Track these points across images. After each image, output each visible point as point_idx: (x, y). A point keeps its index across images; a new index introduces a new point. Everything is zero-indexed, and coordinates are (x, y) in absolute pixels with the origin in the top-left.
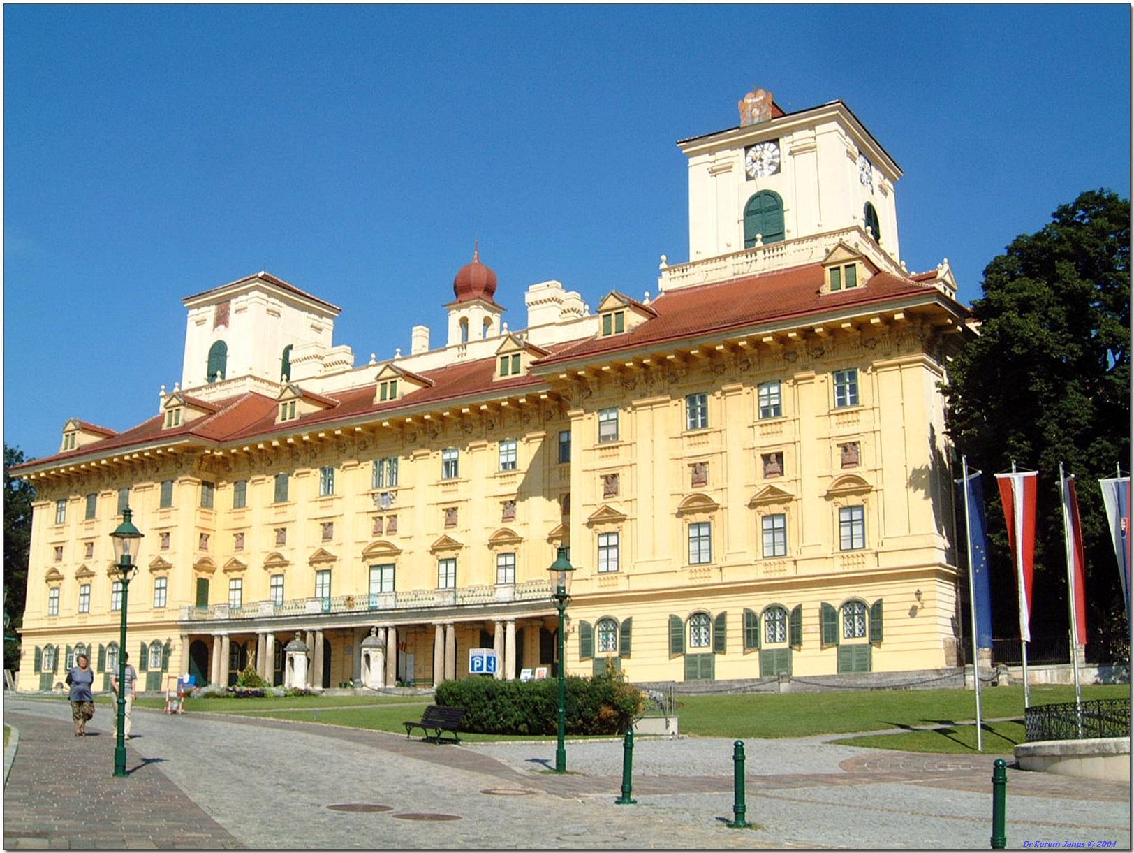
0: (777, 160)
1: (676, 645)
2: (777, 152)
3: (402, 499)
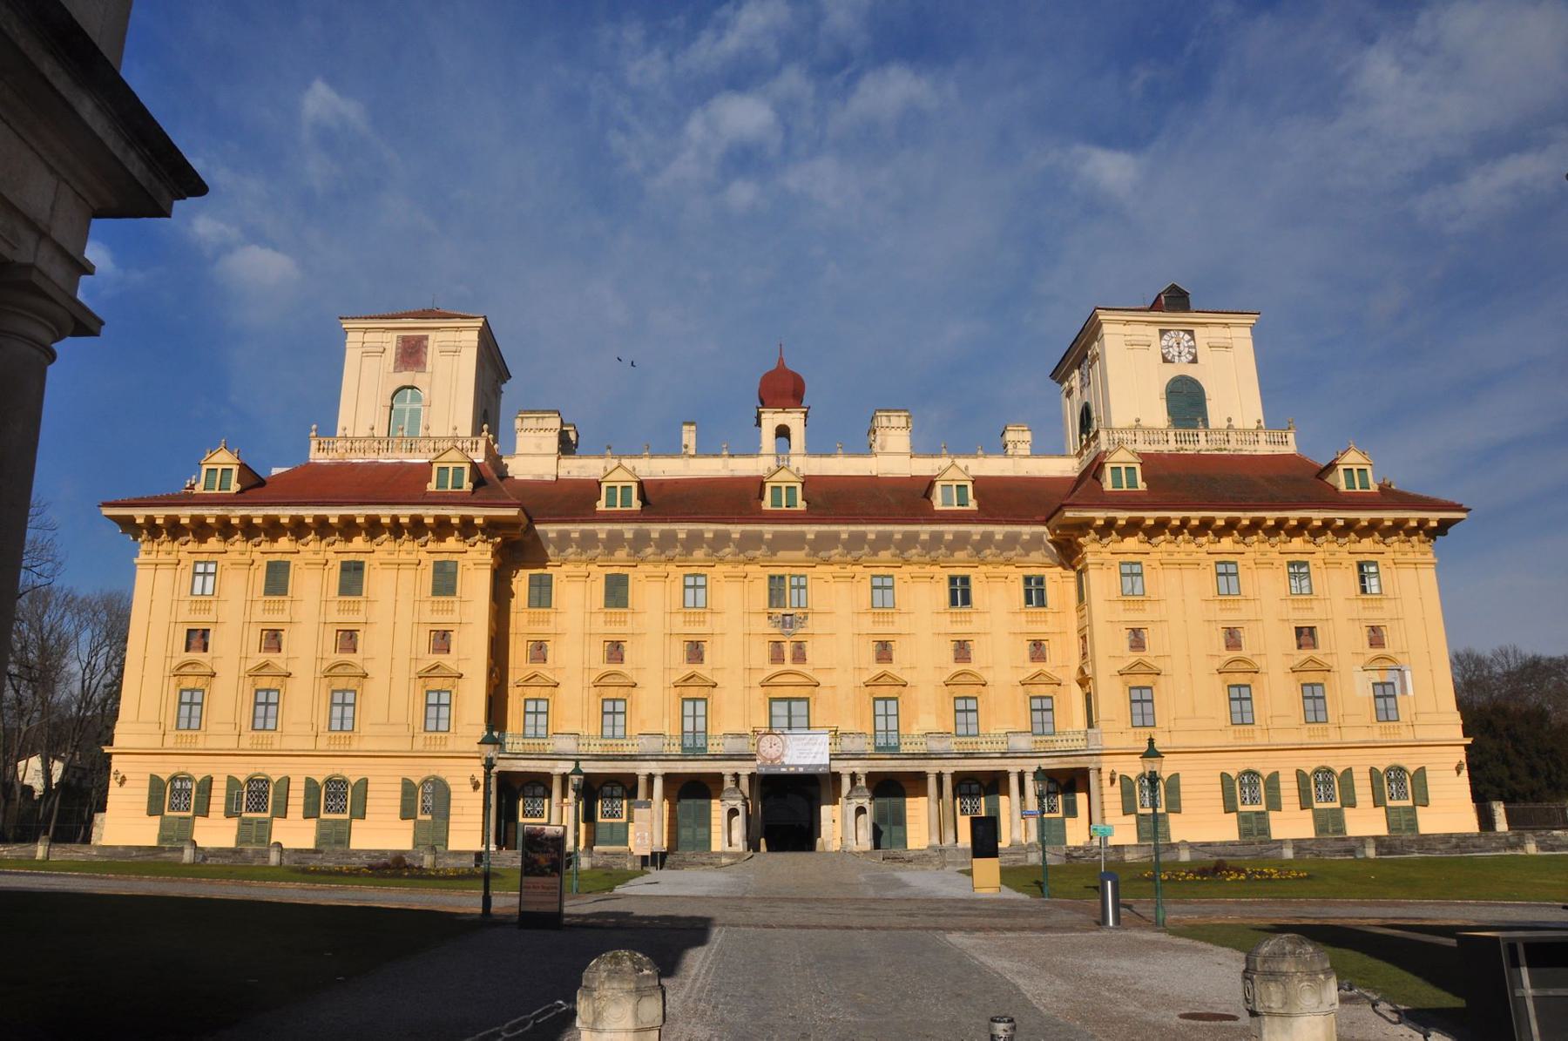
2: (1192, 343)
3: (813, 625)
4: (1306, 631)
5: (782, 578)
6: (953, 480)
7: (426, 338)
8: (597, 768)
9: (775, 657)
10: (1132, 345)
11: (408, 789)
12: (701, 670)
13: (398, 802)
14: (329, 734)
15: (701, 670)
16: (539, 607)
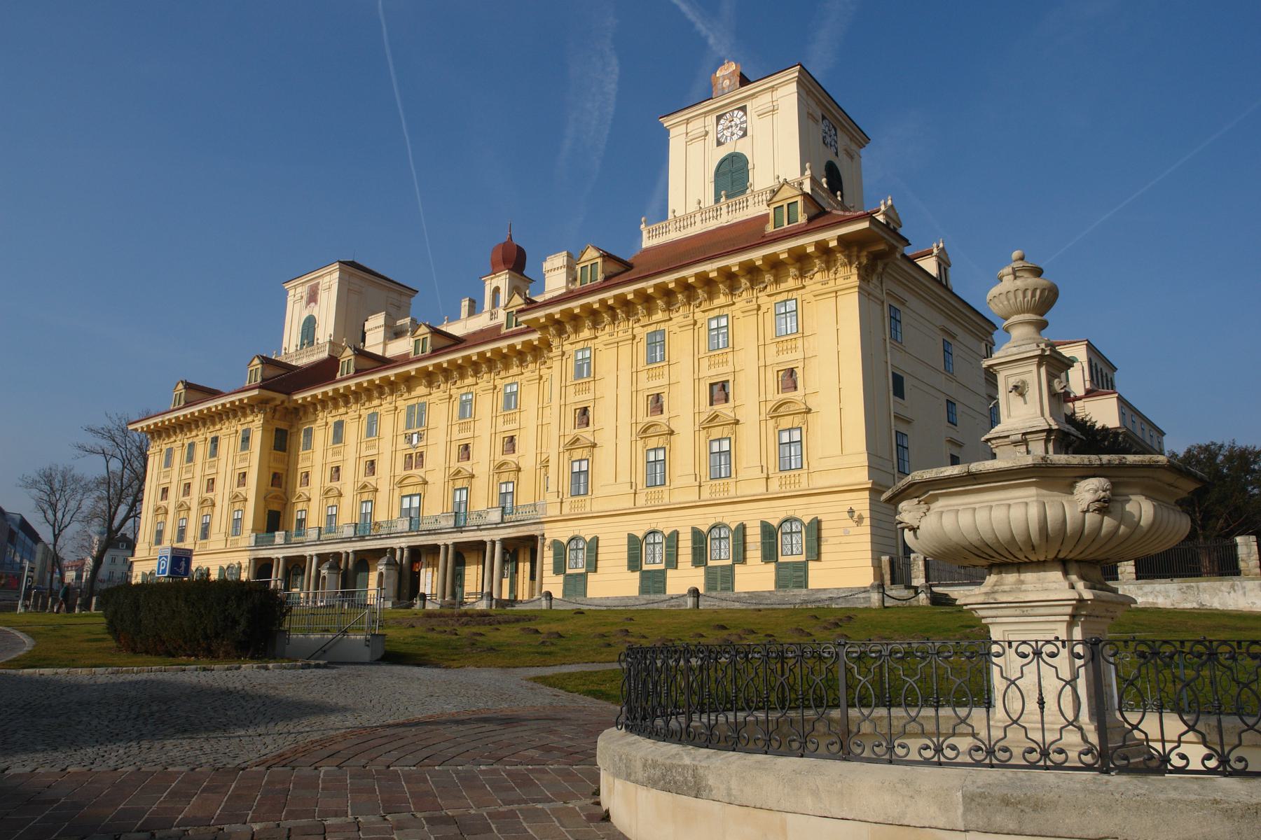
0: (744, 126)
1: (634, 562)
2: (744, 118)
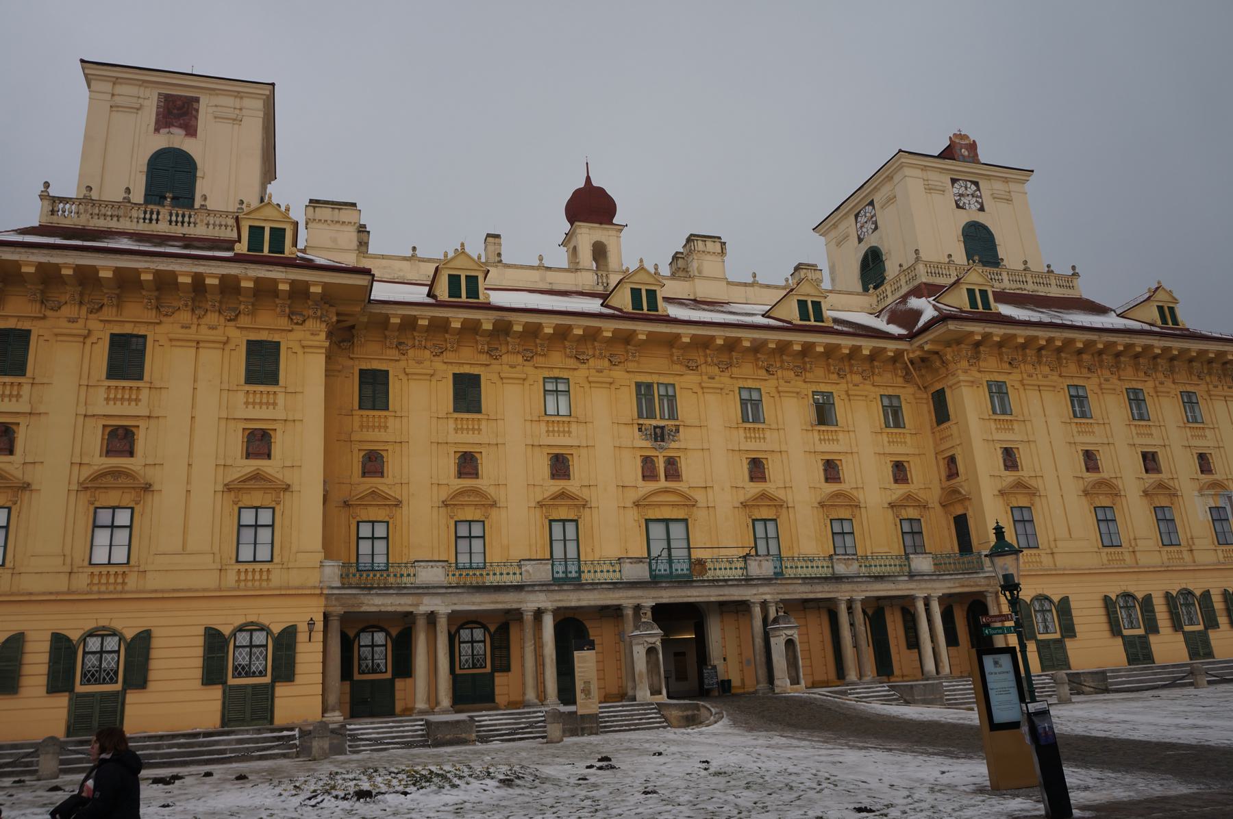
3: (687, 438)
4: (1150, 456)
5: (649, 386)
6: (808, 295)
7: (197, 100)
8: (474, 604)
9: (648, 474)
10: (930, 189)
11: (215, 643)
12: (572, 486)
13: (199, 662)
14: (91, 569)
15: (572, 486)
16: (374, 409)
